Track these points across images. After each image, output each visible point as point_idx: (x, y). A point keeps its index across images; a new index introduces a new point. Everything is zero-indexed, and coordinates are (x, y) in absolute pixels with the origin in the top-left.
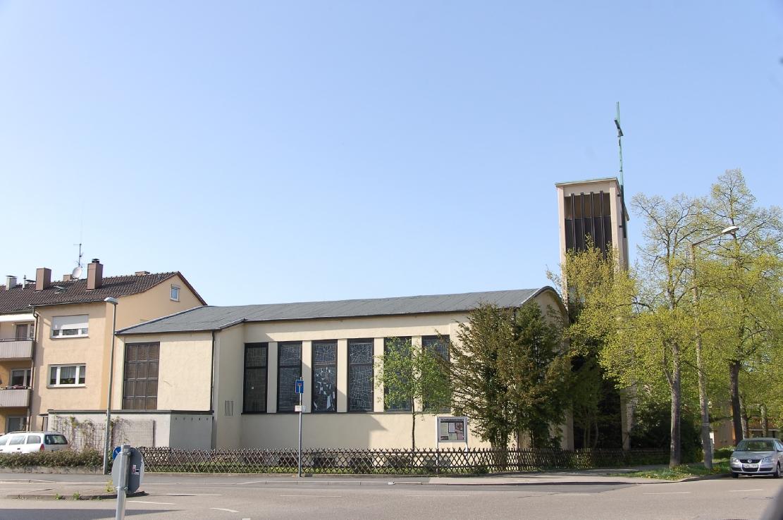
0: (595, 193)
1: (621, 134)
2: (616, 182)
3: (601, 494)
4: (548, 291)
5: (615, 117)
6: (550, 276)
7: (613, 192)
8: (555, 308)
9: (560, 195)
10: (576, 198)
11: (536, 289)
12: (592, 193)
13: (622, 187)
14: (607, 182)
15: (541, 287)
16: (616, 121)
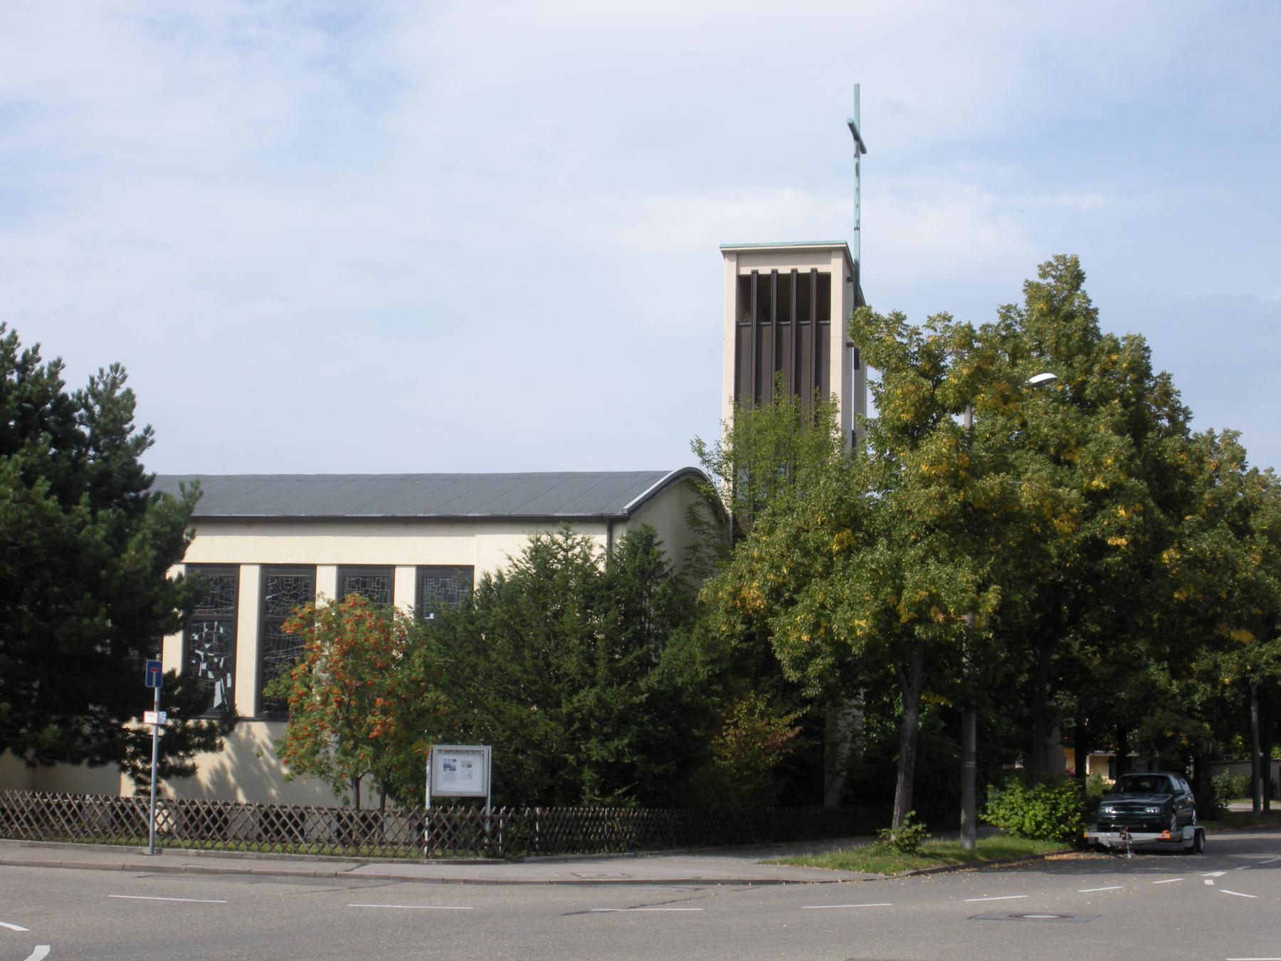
0: (761, 272)
1: (861, 149)
2: (845, 251)
3: (265, 888)
4: (689, 479)
5: (851, 116)
6: (699, 449)
7: (835, 268)
8: (705, 514)
9: (725, 279)
10: (763, 280)
11: (666, 473)
12: (774, 272)
13: (857, 264)
14: (825, 252)
15: (674, 467)
16: (852, 126)
